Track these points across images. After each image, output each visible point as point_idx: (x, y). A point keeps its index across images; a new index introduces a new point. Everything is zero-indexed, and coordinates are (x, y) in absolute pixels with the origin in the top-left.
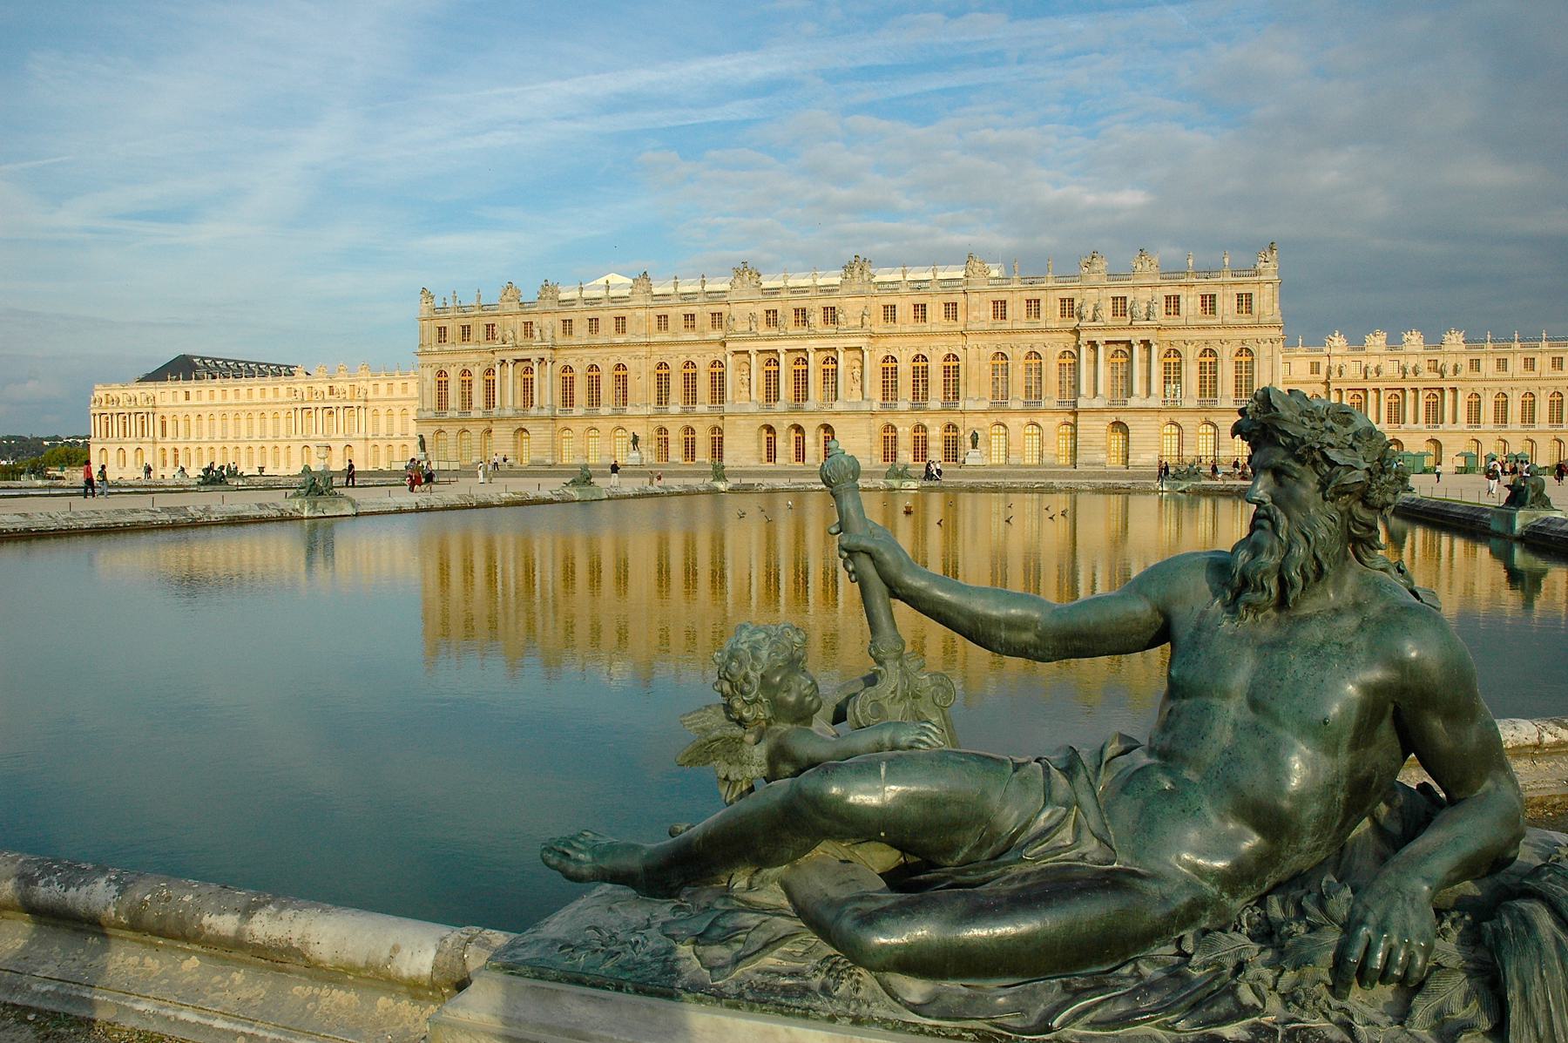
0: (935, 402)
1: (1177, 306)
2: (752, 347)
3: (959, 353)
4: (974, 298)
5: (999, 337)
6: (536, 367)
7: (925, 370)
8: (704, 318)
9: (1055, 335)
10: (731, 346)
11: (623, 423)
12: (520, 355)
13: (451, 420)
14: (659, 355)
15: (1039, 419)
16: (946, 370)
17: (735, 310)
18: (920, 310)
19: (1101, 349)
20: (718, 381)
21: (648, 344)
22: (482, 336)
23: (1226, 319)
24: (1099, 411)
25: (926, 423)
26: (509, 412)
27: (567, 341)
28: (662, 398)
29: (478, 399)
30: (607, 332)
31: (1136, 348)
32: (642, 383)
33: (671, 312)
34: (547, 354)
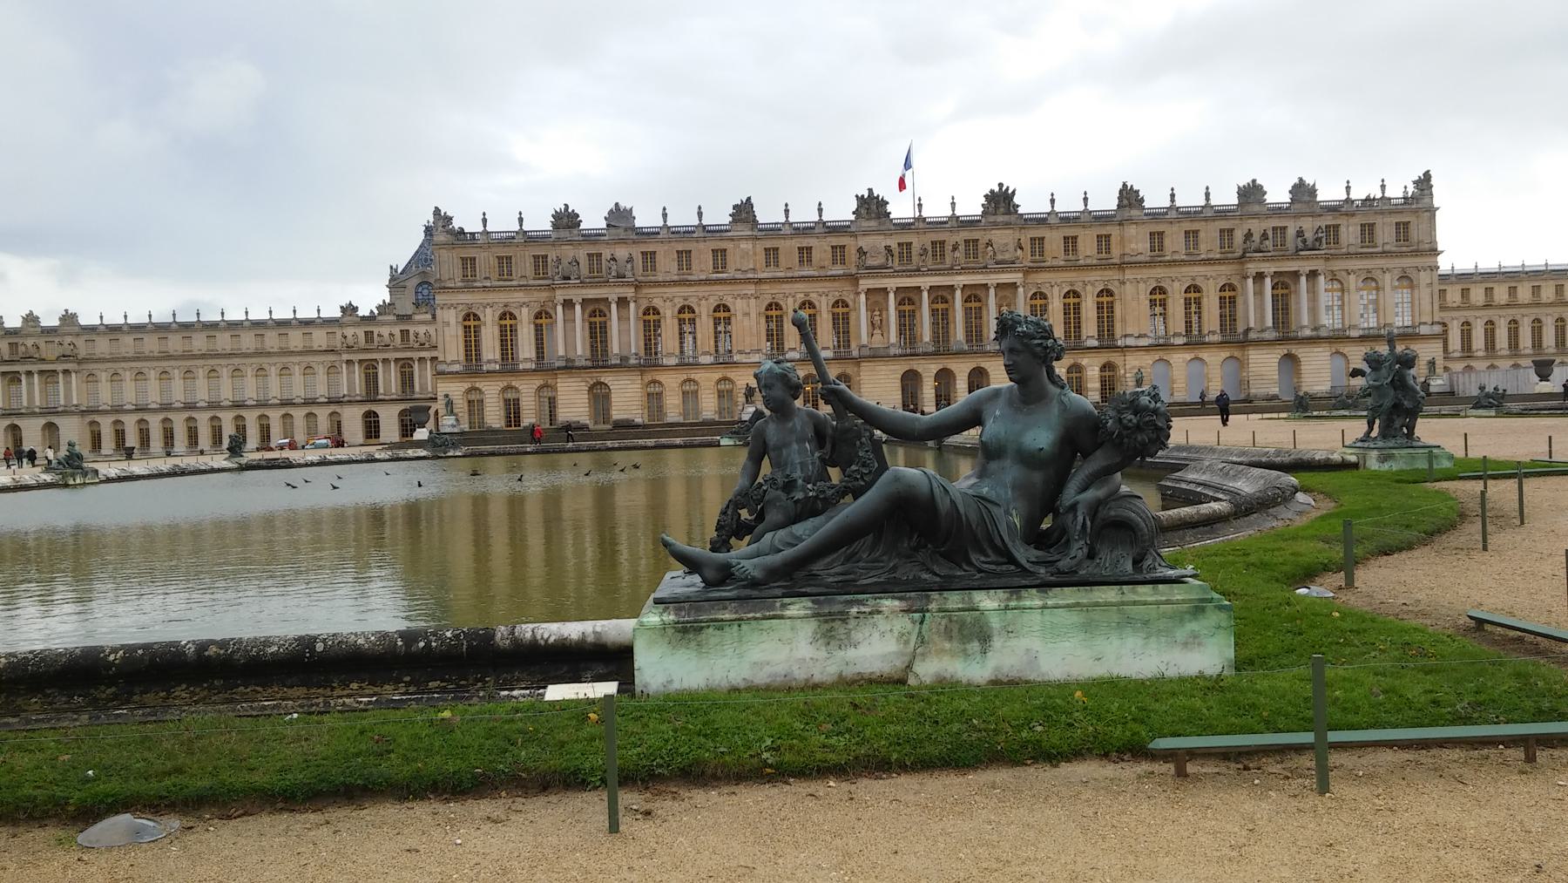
1: (1337, 235)
4: (1131, 230)
5: (1159, 270)
6: (614, 307)
7: (1077, 307)
8: (821, 248)
9: (1216, 268)
10: (865, 284)
11: (731, 374)
12: (592, 293)
14: (769, 293)
15: (1204, 355)
16: (1100, 307)
17: (864, 242)
18: (1070, 243)
19: (1268, 281)
20: (842, 323)
21: (760, 281)
22: (530, 271)
23: (1387, 248)
25: (1084, 362)
29: (526, 349)
30: (702, 265)
31: (1303, 279)
33: (782, 244)
34: (629, 292)
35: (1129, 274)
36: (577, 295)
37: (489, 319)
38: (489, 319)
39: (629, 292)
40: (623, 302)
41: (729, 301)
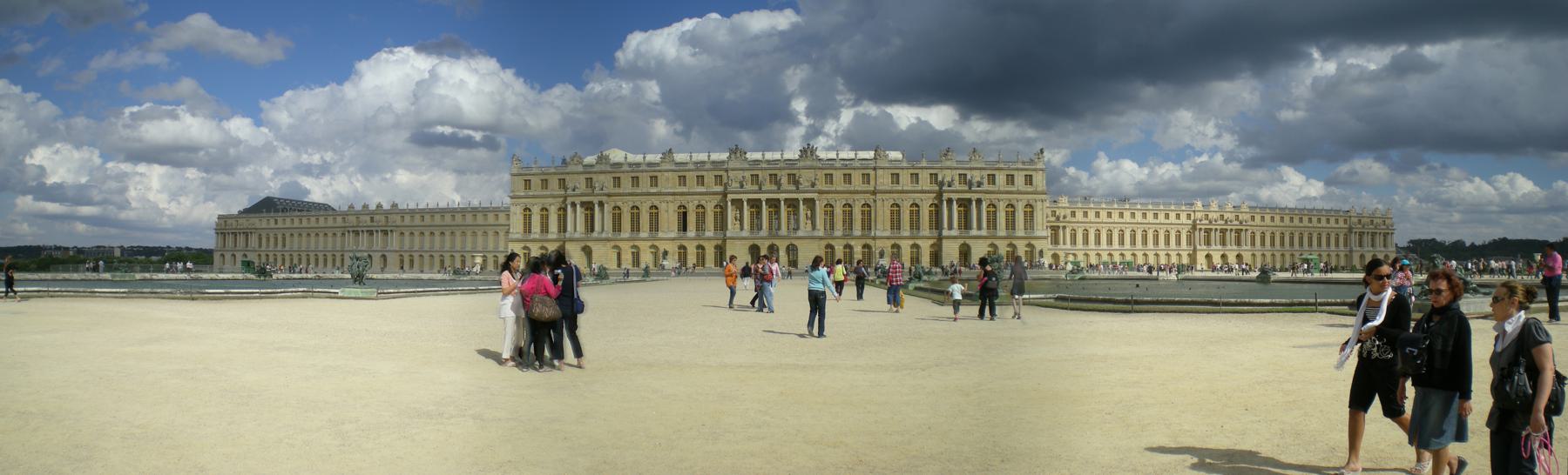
0: (857, 232)
2: (744, 197)
3: (871, 202)
4: (880, 172)
7: (851, 213)
8: (709, 177)
12: (585, 199)
13: (534, 240)
21: (674, 194)
24: (955, 238)
25: (852, 243)
26: (577, 235)
27: (617, 190)
28: (684, 227)
32: (669, 218)
34: (604, 199)
35: (879, 196)
36: (577, 201)
37: (536, 211)
38: (536, 211)
39: (604, 199)
40: (601, 204)
41: (656, 203)
